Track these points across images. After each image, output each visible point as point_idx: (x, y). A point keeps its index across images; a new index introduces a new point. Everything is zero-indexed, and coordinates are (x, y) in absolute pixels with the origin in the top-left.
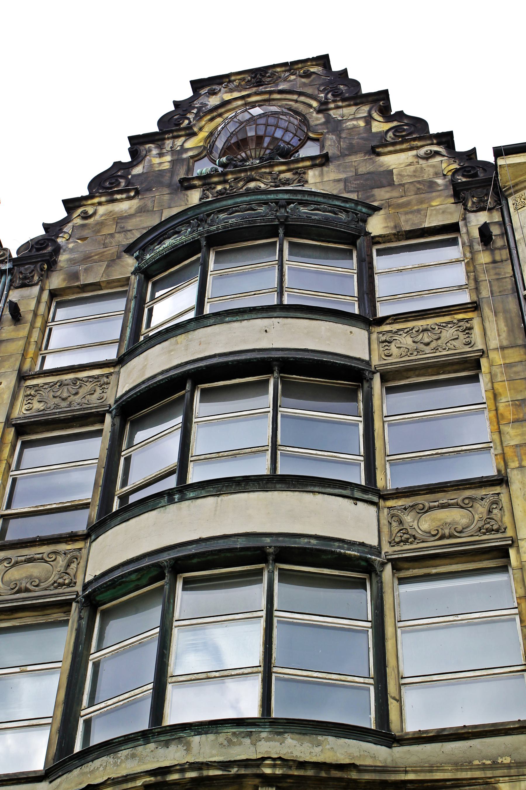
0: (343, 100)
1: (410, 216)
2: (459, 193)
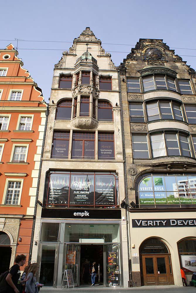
0: (167, 50)
1: (182, 76)
2: (190, 74)
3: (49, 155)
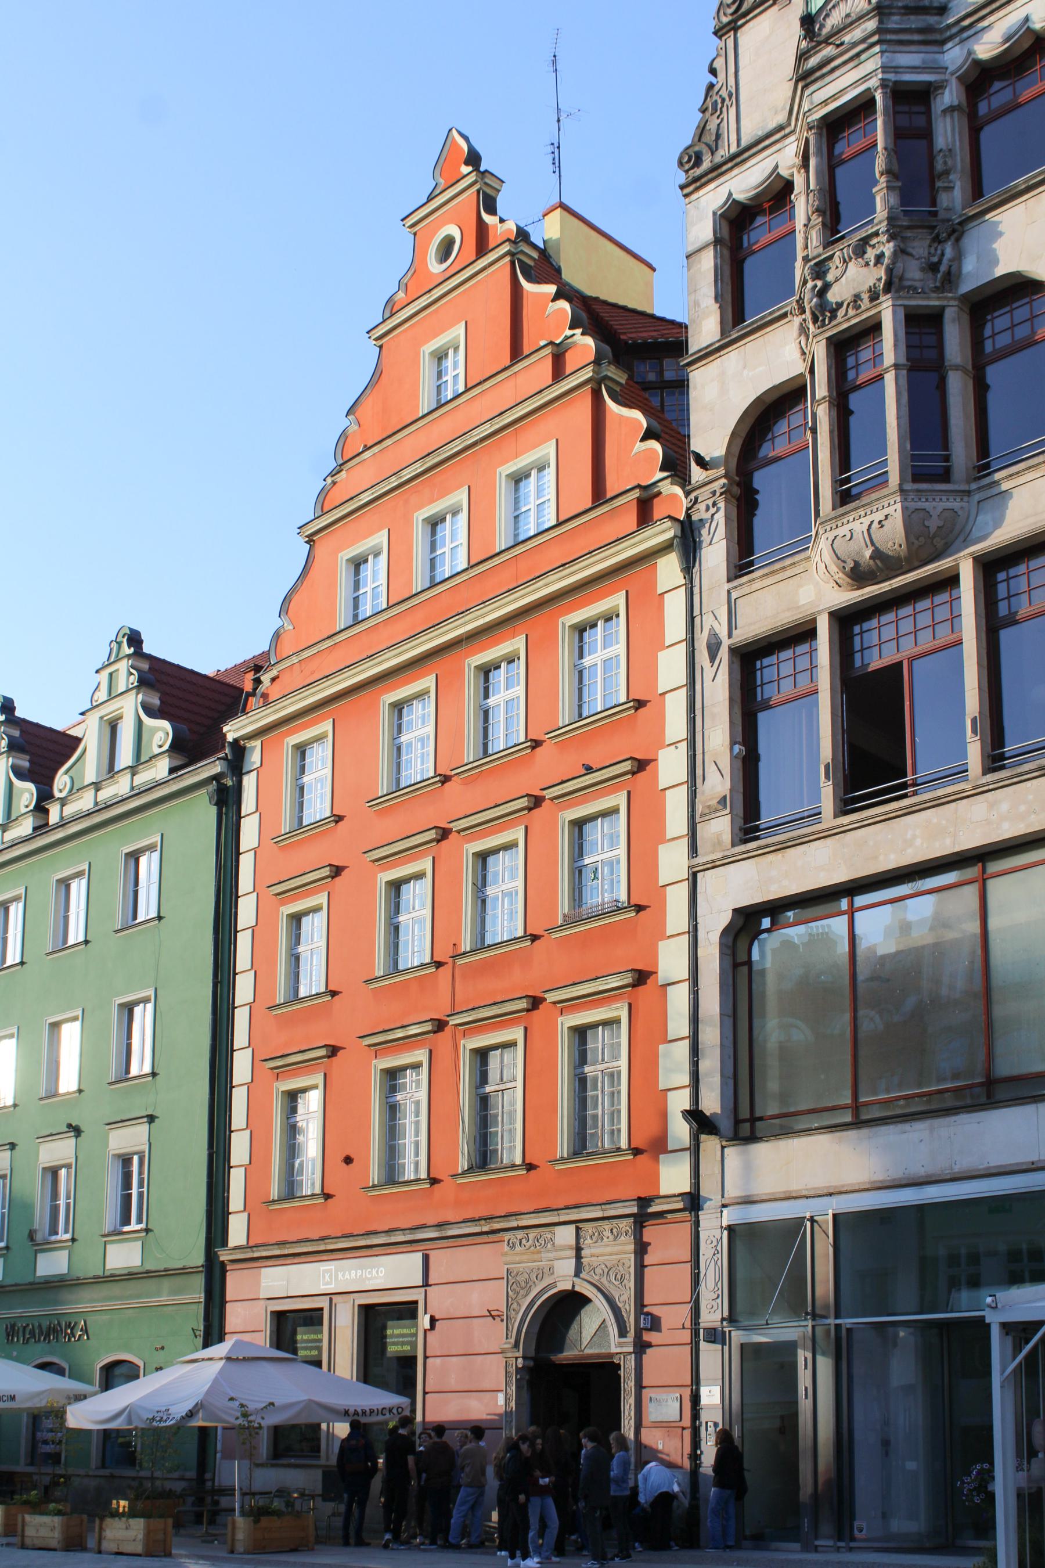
3: (719, 828)
